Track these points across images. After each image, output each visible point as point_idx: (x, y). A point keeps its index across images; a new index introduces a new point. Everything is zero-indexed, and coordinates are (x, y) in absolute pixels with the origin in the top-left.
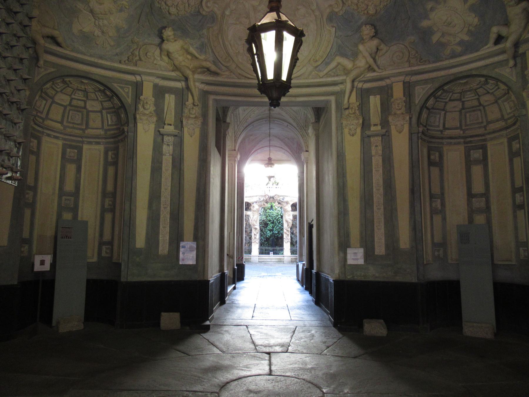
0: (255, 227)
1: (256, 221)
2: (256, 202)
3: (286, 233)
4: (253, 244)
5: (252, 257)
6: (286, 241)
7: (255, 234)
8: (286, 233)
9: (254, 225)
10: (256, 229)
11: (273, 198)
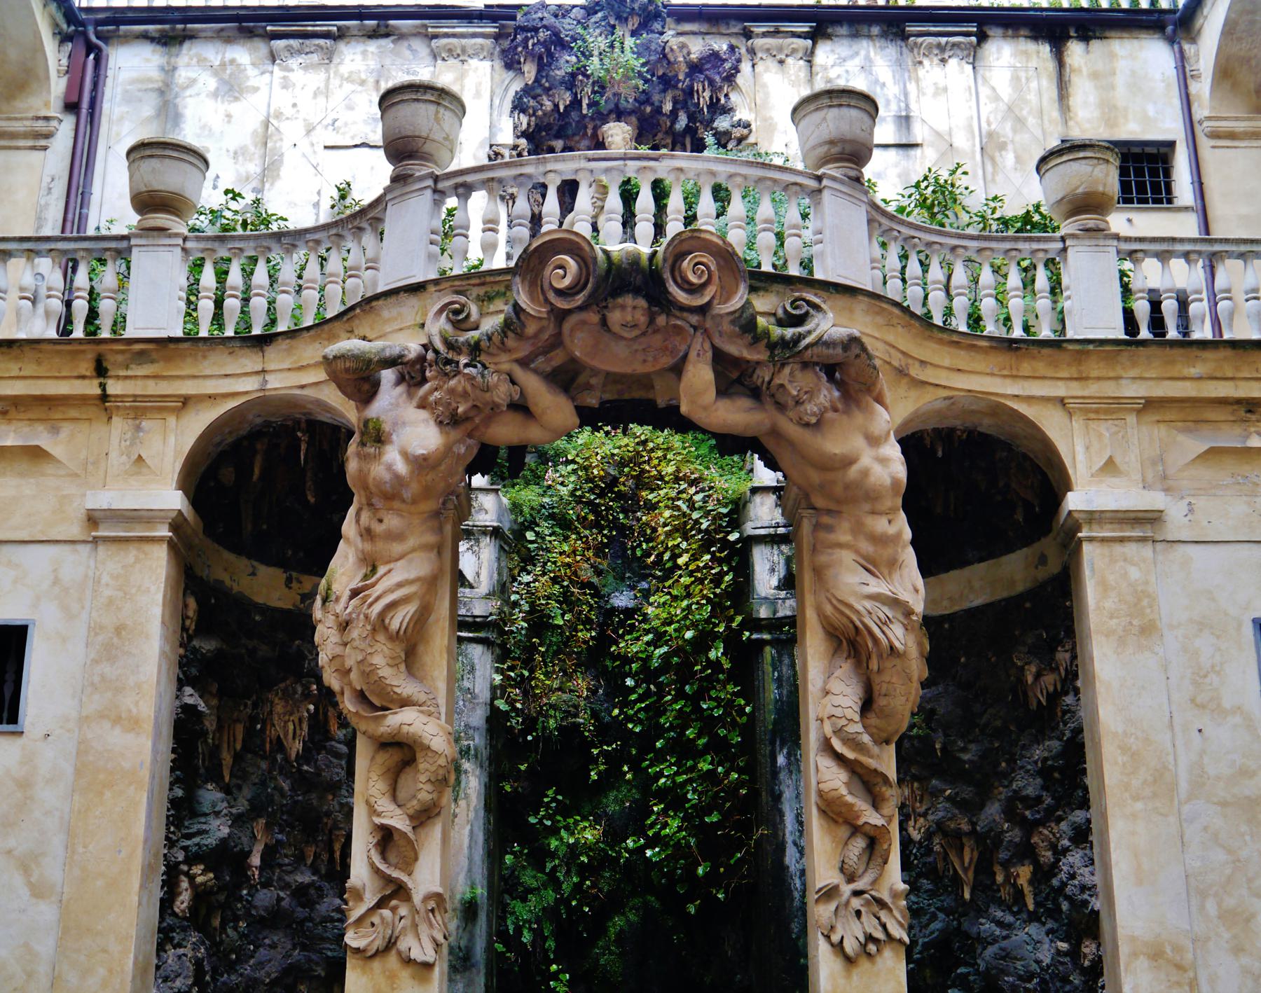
1: (410, 649)
2: (413, 373)
3: (834, 812)
6: (851, 933)
9: (378, 700)
10: (403, 753)
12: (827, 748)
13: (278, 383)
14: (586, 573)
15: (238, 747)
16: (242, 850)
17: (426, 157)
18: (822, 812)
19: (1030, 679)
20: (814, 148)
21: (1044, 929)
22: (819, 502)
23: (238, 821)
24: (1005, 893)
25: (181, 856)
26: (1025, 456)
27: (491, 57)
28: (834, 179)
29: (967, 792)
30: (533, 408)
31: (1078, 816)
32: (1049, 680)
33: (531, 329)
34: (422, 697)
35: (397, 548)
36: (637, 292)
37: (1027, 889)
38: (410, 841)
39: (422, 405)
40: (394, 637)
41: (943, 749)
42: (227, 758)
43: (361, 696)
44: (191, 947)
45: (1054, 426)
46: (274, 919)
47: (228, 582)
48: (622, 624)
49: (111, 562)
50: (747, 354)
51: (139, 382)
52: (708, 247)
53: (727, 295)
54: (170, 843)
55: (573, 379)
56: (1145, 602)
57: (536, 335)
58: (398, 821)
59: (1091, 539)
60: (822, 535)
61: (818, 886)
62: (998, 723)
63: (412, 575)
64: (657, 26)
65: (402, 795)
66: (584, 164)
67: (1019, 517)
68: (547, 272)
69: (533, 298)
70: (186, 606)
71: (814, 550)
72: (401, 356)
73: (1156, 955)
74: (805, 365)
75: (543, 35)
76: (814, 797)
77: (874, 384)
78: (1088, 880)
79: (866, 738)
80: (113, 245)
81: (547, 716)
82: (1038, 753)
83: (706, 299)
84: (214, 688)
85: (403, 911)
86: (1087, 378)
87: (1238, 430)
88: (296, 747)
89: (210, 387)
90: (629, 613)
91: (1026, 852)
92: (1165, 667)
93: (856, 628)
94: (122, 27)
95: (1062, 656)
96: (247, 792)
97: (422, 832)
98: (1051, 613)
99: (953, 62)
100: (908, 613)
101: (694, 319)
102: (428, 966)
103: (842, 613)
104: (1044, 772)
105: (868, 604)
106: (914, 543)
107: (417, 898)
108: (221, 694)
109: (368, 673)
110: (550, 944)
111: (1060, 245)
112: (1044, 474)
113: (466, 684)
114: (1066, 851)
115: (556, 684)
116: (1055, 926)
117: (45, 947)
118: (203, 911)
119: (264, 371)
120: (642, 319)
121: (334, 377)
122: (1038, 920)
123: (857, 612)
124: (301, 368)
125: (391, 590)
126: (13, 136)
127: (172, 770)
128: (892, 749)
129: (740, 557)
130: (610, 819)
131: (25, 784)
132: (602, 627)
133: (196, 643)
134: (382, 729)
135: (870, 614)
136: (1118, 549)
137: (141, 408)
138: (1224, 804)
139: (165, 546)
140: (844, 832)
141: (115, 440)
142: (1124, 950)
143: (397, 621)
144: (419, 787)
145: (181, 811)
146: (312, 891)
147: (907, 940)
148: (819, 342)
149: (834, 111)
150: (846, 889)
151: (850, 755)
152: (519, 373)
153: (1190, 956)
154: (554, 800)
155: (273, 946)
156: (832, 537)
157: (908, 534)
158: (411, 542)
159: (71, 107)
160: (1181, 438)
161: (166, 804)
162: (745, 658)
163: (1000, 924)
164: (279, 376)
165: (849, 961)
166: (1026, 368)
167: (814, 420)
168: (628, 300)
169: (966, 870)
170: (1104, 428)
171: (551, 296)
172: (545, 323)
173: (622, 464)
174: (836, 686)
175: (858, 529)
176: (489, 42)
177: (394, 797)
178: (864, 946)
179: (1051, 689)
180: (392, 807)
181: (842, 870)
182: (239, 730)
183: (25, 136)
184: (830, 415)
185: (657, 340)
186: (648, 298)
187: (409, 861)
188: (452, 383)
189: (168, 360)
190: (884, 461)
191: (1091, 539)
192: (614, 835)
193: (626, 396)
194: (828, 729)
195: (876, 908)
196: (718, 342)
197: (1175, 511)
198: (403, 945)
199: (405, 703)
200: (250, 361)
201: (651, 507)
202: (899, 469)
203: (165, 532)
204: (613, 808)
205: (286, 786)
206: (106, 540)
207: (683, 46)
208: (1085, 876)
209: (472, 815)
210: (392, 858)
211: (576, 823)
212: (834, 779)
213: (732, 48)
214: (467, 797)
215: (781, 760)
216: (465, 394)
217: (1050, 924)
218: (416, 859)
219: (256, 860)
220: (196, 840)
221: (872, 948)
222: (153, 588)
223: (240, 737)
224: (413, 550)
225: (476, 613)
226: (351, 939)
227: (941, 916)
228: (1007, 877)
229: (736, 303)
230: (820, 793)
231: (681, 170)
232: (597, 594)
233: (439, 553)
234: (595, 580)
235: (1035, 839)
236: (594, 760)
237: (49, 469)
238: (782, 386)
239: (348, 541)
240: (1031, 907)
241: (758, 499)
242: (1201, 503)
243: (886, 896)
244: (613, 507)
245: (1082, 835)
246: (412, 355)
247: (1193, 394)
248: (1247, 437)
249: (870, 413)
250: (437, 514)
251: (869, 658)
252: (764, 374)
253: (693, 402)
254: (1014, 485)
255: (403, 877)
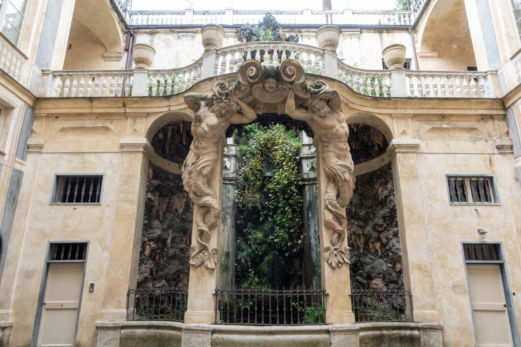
0: (208, 199)
2: (210, 103)
3: (328, 226)
4: (192, 273)
5: (184, 336)
6: (334, 261)
7: (201, 233)
8: (328, 226)
9: (199, 194)
10: (206, 209)
11: (276, 75)
12: (327, 208)
13: (173, 109)
14: (259, 168)
15: (165, 210)
16: (165, 239)
17: (214, 45)
18: (326, 226)
19: (380, 192)
20: (322, 43)
21: (384, 261)
22: (324, 139)
23: (164, 230)
24: (373, 251)
25: (147, 239)
26: (379, 131)
27: (235, 37)
28: (328, 50)
29: (361, 223)
30: (243, 112)
31: (395, 229)
32: (386, 193)
33: (243, 88)
34: (212, 193)
35: (205, 152)
36: (273, 77)
37: (379, 250)
38: (208, 234)
39: (212, 112)
40: (204, 176)
41: (355, 212)
42: (161, 213)
43: (195, 193)
44: (150, 264)
45: (388, 121)
46: (174, 257)
47: (162, 166)
48: (268, 180)
49: (127, 158)
50: (304, 96)
51: (135, 109)
52: (293, 64)
53: (298, 78)
54: (143, 235)
55: (255, 106)
56: (414, 170)
57: (244, 91)
58: (205, 228)
59: (399, 152)
60: (325, 148)
61: (325, 247)
62: (370, 205)
63: (209, 159)
64: (277, 30)
65: (206, 221)
66: (258, 45)
67: (376, 148)
68: (247, 72)
69: (243, 80)
70: (149, 171)
71: (323, 153)
72: (206, 97)
73: (420, 268)
74: (321, 99)
75: (248, 31)
76: (323, 222)
77: (340, 106)
78: (398, 247)
79: (338, 205)
80: (129, 72)
81: (249, 203)
82: (382, 212)
83: (293, 79)
84: (158, 194)
85: (206, 254)
86: (397, 108)
87: (439, 123)
88: (181, 211)
89: (155, 110)
90: (270, 177)
91: (379, 239)
92: (421, 187)
93: (335, 174)
94: (140, 30)
95: (389, 186)
96: (167, 222)
97: (212, 231)
98: (386, 174)
99: (354, 39)
100: (350, 170)
101: (289, 86)
102: (213, 270)
103: (331, 170)
104: (384, 218)
105: (339, 167)
106: (350, 151)
107: (210, 250)
108: (160, 195)
109: (197, 186)
110: (249, 263)
111: (389, 73)
112: (384, 136)
113: (227, 195)
114: (391, 239)
115: (251, 196)
116: (387, 260)
117: (106, 264)
118: (154, 255)
119: (170, 106)
120: (274, 86)
121: (186, 102)
122: (382, 258)
123: (336, 169)
124: (180, 105)
125: (203, 163)
126: (111, 57)
127: (144, 215)
128: (345, 209)
129: (299, 164)
130: (265, 231)
131: (101, 219)
132: (263, 181)
133: (152, 181)
134: (201, 202)
135: (339, 170)
136: (407, 155)
137: (135, 116)
138: (438, 226)
139: (142, 153)
140: (331, 232)
141: (128, 125)
142: (410, 267)
143: (205, 171)
144: (211, 219)
145: (147, 227)
146: (185, 249)
147: (350, 263)
148: (325, 92)
149: (328, 32)
150: (332, 248)
151: (334, 210)
152: (240, 102)
153: (429, 268)
154: (250, 226)
155: (174, 264)
156: (328, 149)
157: (349, 149)
158: (209, 150)
159: (127, 50)
160: (423, 125)
161: (142, 225)
162: (301, 189)
163: (371, 259)
164: (174, 107)
165: (333, 269)
166: (380, 105)
167: (323, 115)
168: (271, 80)
169: (361, 244)
170: (402, 122)
171: (248, 79)
172: (247, 87)
173: (268, 140)
174: (329, 190)
175: (335, 146)
176: (234, 34)
177: (204, 221)
178: (338, 265)
179: (386, 195)
180: (203, 224)
181: (331, 243)
182: (165, 206)
183: (115, 57)
184: (327, 114)
185: (278, 93)
186: (277, 79)
187: (208, 240)
188: (221, 104)
189: (143, 103)
190: (343, 127)
191: (399, 152)
192: (266, 236)
193: (270, 112)
194: (327, 203)
195: (341, 254)
196: (296, 92)
197: (423, 145)
198: (206, 264)
199: (207, 195)
200: (166, 103)
201: (276, 150)
202: (347, 130)
203: (142, 150)
204: (266, 228)
205: (178, 221)
206: (125, 152)
207: (284, 34)
208: (397, 246)
209: (228, 229)
210: (203, 239)
211: (256, 232)
212: (329, 217)
213: (297, 35)
214: (227, 225)
215: (310, 215)
216: (224, 108)
217: (386, 259)
218: (210, 239)
219: (169, 241)
220: (151, 235)
221: (340, 265)
222: (138, 165)
223: (165, 208)
224: (210, 152)
225: (230, 177)
226: (192, 262)
227: (354, 257)
228: (373, 247)
229: (302, 81)
230: (325, 221)
231: (285, 47)
232: (262, 172)
233: (217, 154)
234: (261, 169)
235: (381, 236)
236: (261, 215)
237: (110, 133)
238: (314, 105)
239: (192, 150)
240: (380, 255)
241: (304, 148)
242: (429, 142)
243: (343, 250)
244: (266, 152)
245: (396, 235)
246: (209, 97)
247: (427, 113)
248: (442, 125)
249: (339, 115)
250: (217, 143)
251: (339, 182)
252: (309, 102)
253: (289, 110)
254: (375, 140)
255: (206, 244)
